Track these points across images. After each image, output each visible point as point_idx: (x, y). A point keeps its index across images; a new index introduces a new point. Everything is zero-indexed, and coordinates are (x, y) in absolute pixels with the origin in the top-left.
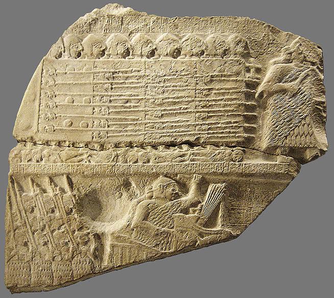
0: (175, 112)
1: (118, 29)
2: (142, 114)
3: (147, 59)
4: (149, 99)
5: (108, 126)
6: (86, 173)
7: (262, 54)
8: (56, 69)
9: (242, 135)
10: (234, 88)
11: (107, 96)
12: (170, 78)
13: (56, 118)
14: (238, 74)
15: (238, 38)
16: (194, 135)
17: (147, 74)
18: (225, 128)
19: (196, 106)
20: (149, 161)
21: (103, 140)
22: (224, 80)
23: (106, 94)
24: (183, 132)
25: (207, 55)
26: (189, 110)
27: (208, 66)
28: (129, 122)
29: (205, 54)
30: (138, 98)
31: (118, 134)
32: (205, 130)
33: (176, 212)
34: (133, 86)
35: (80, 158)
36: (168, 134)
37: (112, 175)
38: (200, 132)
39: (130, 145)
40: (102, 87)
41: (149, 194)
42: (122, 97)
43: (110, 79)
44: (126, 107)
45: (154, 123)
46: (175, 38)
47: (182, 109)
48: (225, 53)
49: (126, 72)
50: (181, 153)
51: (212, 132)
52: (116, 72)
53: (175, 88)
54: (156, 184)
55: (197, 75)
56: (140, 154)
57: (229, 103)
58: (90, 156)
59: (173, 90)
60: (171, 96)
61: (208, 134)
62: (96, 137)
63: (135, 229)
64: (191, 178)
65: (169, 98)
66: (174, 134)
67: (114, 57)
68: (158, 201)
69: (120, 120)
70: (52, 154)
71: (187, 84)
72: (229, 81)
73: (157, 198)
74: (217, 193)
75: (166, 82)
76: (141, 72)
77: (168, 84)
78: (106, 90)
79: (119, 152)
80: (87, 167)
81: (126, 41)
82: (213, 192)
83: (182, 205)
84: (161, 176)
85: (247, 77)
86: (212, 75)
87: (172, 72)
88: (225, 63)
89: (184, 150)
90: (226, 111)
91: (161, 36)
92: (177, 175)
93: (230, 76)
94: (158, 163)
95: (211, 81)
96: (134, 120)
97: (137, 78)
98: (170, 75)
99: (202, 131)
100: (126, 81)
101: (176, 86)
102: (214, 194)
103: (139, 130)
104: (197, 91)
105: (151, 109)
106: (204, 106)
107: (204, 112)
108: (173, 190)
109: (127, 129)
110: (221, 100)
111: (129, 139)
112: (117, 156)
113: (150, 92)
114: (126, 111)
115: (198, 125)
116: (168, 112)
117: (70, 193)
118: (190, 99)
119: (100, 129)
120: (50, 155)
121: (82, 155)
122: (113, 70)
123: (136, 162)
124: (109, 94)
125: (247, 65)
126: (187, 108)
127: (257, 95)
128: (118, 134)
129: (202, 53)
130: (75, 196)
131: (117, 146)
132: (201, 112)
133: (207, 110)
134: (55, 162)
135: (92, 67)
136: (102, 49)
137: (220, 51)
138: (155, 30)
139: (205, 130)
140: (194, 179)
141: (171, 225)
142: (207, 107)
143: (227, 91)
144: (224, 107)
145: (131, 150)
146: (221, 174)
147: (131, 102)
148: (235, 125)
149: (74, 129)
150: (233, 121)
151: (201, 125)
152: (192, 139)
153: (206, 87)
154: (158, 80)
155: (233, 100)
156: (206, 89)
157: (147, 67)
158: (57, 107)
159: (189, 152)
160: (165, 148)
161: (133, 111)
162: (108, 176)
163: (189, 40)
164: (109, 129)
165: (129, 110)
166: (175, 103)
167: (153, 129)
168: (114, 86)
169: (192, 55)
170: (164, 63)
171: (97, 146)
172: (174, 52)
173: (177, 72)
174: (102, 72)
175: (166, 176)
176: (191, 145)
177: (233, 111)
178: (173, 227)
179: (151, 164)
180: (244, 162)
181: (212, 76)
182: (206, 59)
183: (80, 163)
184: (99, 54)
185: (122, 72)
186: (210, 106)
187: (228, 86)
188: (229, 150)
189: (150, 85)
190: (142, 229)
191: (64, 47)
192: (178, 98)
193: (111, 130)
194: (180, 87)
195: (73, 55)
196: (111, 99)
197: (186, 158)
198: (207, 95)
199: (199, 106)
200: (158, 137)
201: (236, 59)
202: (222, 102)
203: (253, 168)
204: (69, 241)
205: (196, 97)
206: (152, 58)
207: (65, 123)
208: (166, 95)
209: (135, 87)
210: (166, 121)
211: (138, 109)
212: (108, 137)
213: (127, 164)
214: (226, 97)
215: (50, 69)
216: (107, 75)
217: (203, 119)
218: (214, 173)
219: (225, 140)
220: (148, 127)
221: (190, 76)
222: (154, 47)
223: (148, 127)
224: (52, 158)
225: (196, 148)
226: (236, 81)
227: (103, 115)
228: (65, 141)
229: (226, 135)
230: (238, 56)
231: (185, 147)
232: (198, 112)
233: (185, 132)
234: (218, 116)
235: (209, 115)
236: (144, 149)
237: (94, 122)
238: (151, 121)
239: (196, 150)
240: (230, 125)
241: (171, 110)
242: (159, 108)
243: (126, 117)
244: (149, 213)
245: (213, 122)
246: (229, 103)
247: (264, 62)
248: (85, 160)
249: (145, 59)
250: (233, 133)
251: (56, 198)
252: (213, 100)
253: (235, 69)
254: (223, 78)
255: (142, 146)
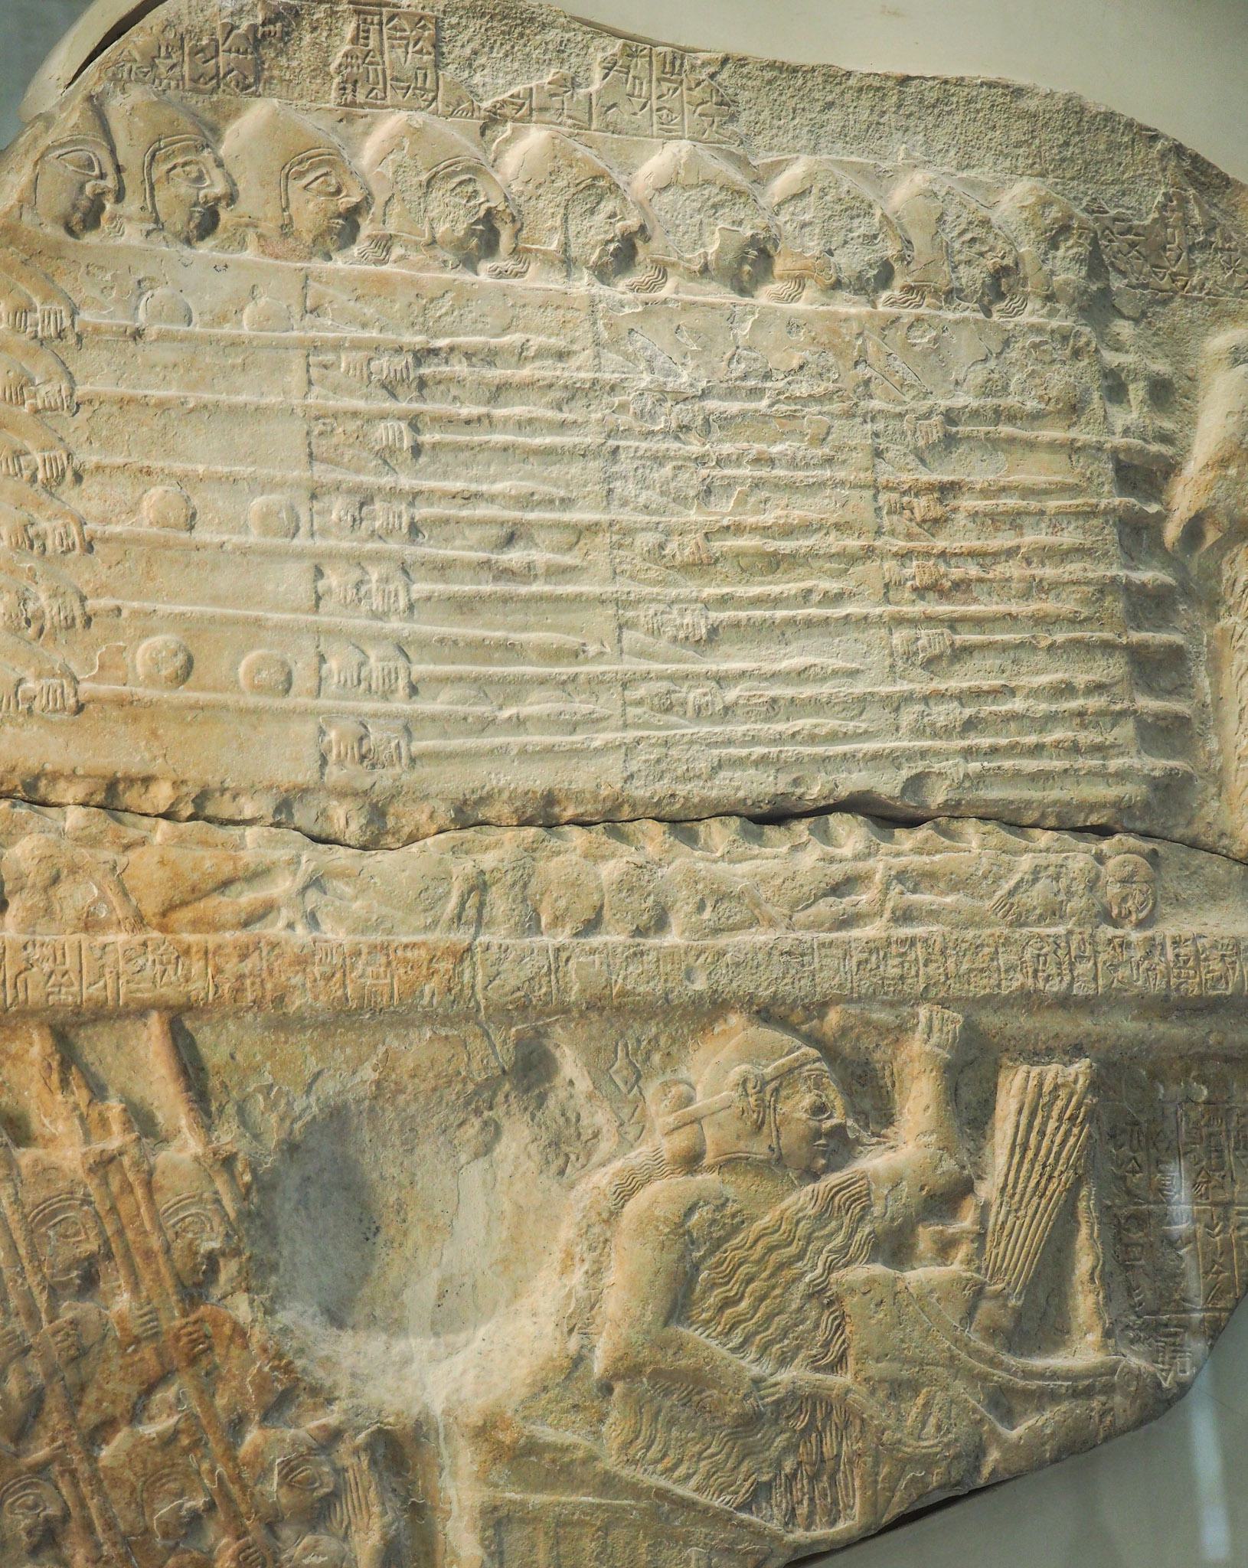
0: (780, 614)
1: (417, 90)
2: (602, 620)
3: (600, 290)
4: (628, 531)
5: (413, 690)
6: (296, 1002)
7: (1165, 302)
8: (76, 299)
9: (1136, 763)
10: (1065, 489)
11: (394, 493)
12: (734, 407)
13: (88, 621)
14: (1074, 409)
15: (1054, 212)
16: (894, 759)
17: (608, 377)
18: (1050, 720)
19: (887, 585)
20: (660, 922)
21: (385, 778)
22: (1011, 440)
23: (387, 481)
24: (833, 737)
25: (910, 289)
26: (851, 609)
27: (925, 355)
28: (529, 670)
29: (898, 281)
30: (568, 517)
31: (471, 743)
32: (947, 732)
33: (845, 1257)
34: (538, 441)
35: (247, 897)
36: (759, 751)
37: (458, 1012)
38: (927, 743)
39: (544, 815)
40: (361, 438)
41: (681, 1141)
42: (482, 511)
43: (400, 390)
44: (506, 573)
45: (672, 678)
46: (739, 179)
47: (815, 597)
48: (1001, 284)
49: (490, 357)
50: (837, 872)
51: (985, 742)
52: (434, 352)
53: (764, 472)
54: (717, 1070)
55: (876, 404)
56: (610, 871)
57: (1049, 572)
58: (316, 882)
59: (757, 484)
60: (751, 520)
61: (968, 753)
62: (340, 762)
63: (619, 1388)
64: (901, 1031)
65: (738, 529)
66: (790, 750)
67: (414, 256)
68: (735, 1188)
69: (480, 650)
70: (74, 869)
71: (827, 450)
72: (1031, 445)
73: (729, 1163)
74: (1052, 1124)
75: (717, 434)
76: (574, 362)
77: (727, 448)
78: (386, 457)
79: (488, 860)
80: (302, 961)
81: (476, 170)
82: (1033, 1115)
83: (877, 1210)
84: (735, 1019)
85: (1119, 429)
86: (949, 410)
87: (745, 377)
88: (1007, 343)
89: (846, 851)
90: (1039, 620)
91: (658, 161)
92: (824, 1005)
93: (1036, 417)
94: (716, 931)
95: (950, 441)
96: (556, 655)
97: (556, 394)
98: (731, 394)
99: (935, 735)
100: (499, 412)
101: (771, 462)
102: (1042, 1133)
103: (593, 722)
104: (883, 498)
105: (647, 590)
106: (927, 588)
107: (929, 620)
108: (819, 1110)
109: (526, 710)
110: (1011, 553)
111: (537, 778)
112: (480, 886)
113: (631, 488)
114: (506, 599)
115: (908, 698)
116: (742, 615)
117: (185, 1147)
118: (853, 543)
119: (369, 706)
120: (56, 880)
121: (258, 874)
122: (418, 340)
123: (592, 925)
124: (406, 482)
125: (1111, 358)
126: (838, 598)
127: (1172, 532)
128: (471, 743)
129: (885, 276)
130: (228, 1162)
131: (467, 816)
132: (913, 622)
133: (944, 609)
134: (89, 923)
135: (296, 310)
136: (344, 202)
137: (974, 276)
138: (621, 116)
139: (947, 732)
140: (919, 1034)
141: (827, 1344)
142: (943, 594)
143: (1033, 505)
144: (1025, 596)
145: (555, 843)
146: (1065, 1002)
147: (531, 542)
148: (1095, 703)
149: (202, 697)
150: (1081, 680)
151: (926, 699)
152: (887, 784)
153: (926, 477)
154: (670, 415)
155: (1064, 555)
156: (930, 488)
157: (605, 335)
158: (89, 548)
159: (879, 866)
160: (745, 834)
161: (558, 599)
162: (428, 1017)
163: (812, 199)
164: (424, 706)
165: (523, 590)
166: (774, 563)
167: (673, 719)
168: (427, 438)
169: (837, 285)
170: (695, 319)
171: (346, 819)
172: (742, 259)
173: (767, 376)
174: (356, 345)
175: (767, 1014)
176: (886, 817)
177: (1074, 621)
178: (840, 1361)
179: (673, 938)
180: (1167, 930)
181: (950, 417)
182: (908, 313)
183: (256, 929)
184: (329, 230)
185: (468, 356)
186: (957, 585)
187: (1036, 471)
188: (1079, 857)
189: (634, 444)
190: (666, 1379)
191: (119, 169)
192: (788, 531)
193: (433, 718)
194: (793, 463)
195: (177, 220)
196: (422, 512)
197: (864, 898)
198: (936, 524)
199: (900, 584)
200: (702, 766)
201: (1054, 323)
202: (1013, 569)
203: (1217, 966)
204: (211, 1507)
205: (879, 532)
206: (623, 284)
207: (148, 653)
208: (723, 510)
209: (548, 454)
210: (735, 666)
211: (570, 589)
212: (413, 760)
213: (538, 941)
214: (1030, 538)
215: (37, 301)
216: (384, 365)
217: (930, 663)
218: (1028, 1000)
219: (1054, 794)
220: (639, 703)
221: (836, 407)
222: (633, 222)
223: (639, 703)
224: (76, 896)
225: (907, 840)
226: (1072, 449)
227: (375, 615)
228: (147, 780)
229: (1058, 764)
230: (1061, 306)
231: (851, 835)
232: (900, 621)
233: (846, 737)
234: (1005, 647)
235: (959, 639)
236: (623, 837)
237: (322, 659)
238: (656, 667)
239: (918, 851)
240: (1074, 704)
241: (757, 602)
242: (689, 588)
243: (516, 637)
244: (696, 1268)
245: (986, 685)
246: (1049, 572)
247: (1176, 344)
248: (285, 915)
249: (583, 284)
250: (1098, 749)
251: (105, 1182)
252: (972, 554)
253: (1058, 379)
254: (1005, 430)
255: (611, 819)
